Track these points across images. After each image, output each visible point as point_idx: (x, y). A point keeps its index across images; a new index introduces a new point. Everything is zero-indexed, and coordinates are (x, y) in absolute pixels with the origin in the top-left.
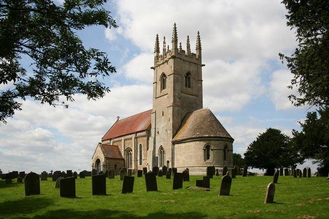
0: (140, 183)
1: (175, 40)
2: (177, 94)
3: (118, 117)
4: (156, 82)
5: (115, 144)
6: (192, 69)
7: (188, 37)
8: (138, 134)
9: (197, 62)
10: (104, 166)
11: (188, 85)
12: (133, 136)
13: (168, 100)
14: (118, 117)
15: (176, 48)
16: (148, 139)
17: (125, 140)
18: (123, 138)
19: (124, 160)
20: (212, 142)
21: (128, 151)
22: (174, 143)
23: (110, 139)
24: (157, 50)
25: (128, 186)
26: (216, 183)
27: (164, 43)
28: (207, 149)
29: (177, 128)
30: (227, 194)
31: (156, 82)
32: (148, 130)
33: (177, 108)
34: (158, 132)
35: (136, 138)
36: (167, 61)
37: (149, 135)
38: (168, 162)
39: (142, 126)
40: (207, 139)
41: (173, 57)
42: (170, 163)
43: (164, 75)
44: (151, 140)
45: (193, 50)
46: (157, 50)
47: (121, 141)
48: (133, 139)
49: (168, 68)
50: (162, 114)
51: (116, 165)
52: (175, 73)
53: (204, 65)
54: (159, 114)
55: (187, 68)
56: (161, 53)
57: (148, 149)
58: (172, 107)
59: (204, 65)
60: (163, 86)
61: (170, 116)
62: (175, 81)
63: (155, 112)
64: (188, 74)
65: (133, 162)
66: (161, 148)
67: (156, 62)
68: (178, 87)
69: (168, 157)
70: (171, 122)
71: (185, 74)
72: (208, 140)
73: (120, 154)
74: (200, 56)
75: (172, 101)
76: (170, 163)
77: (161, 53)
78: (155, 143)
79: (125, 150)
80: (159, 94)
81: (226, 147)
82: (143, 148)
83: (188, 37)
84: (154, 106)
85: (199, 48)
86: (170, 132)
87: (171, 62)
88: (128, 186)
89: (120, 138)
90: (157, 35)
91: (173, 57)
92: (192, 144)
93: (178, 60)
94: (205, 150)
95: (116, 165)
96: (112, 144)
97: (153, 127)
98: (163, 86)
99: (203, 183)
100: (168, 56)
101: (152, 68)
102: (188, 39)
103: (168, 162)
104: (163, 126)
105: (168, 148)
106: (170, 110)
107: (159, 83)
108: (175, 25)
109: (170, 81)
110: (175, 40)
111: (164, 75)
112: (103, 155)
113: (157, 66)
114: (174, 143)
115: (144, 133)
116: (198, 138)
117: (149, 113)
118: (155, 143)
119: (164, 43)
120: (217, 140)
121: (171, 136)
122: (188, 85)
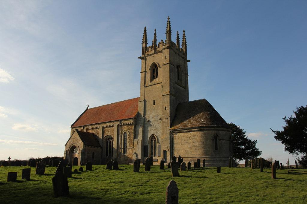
1: (169, 33)
2: (172, 83)
3: (88, 106)
4: (145, 72)
5: (90, 131)
6: (182, 63)
7: (178, 32)
11: (179, 78)
12: (116, 124)
14: (88, 106)
17: (103, 128)
18: (101, 126)
19: (101, 147)
23: (84, 127)
24: (145, 41)
28: (215, 138)
31: (145, 72)
33: (173, 97)
37: (136, 125)
38: (165, 152)
40: (216, 128)
47: (98, 128)
48: (116, 127)
49: (162, 58)
50: (153, 103)
51: (93, 153)
53: (189, 61)
54: (149, 104)
58: (169, 96)
59: (189, 61)
63: (145, 101)
66: (153, 137)
70: (168, 110)
75: (168, 89)
76: (168, 154)
82: (128, 136)
83: (178, 32)
84: (141, 95)
85: (185, 44)
86: (167, 122)
87: (166, 52)
89: (98, 126)
90: (145, 28)
91: (168, 48)
93: (173, 51)
94: (213, 140)
95: (93, 153)
96: (85, 131)
101: (140, 58)
102: (178, 34)
103: (165, 152)
106: (167, 99)
108: (169, 19)
110: (169, 33)
112: (81, 141)
114: (172, 133)
115: (131, 121)
120: (225, 131)
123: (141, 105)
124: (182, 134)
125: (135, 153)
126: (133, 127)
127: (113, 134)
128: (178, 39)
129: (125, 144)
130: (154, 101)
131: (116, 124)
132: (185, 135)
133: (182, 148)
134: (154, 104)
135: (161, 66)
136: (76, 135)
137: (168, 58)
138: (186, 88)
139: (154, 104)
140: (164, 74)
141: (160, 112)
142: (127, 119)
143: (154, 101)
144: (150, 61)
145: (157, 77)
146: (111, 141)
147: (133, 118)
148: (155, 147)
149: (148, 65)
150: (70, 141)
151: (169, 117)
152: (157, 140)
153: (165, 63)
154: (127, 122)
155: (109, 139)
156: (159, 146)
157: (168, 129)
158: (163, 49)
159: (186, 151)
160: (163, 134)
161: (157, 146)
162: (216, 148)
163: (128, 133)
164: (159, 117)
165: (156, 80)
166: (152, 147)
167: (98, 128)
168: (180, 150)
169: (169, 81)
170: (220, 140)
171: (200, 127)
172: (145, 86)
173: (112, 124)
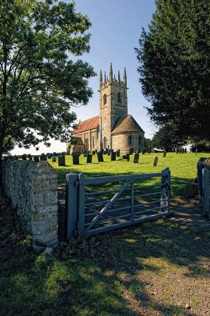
0: (95, 158)
1: (111, 73)
4: (101, 100)
5: (79, 136)
6: (122, 91)
9: (124, 86)
10: (74, 149)
11: (119, 101)
12: (89, 131)
13: (107, 110)
15: (112, 79)
16: (97, 133)
18: (83, 133)
20: (133, 134)
21: (86, 141)
22: (112, 135)
25: (89, 161)
26: (132, 157)
27: (105, 75)
29: (113, 127)
30: (137, 162)
31: (101, 100)
32: (98, 128)
33: (113, 115)
35: (91, 133)
36: (107, 87)
37: (98, 132)
39: (95, 125)
41: (110, 84)
42: (110, 147)
43: (105, 95)
44: (99, 134)
45: (122, 80)
46: (101, 80)
47: (82, 134)
49: (107, 91)
52: (111, 94)
55: (118, 90)
56: (103, 82)
60: (105, 102)
61: (109, 120)
62: (112, 99)
64: (119, 94)
65: (89, 147)
67: (100, 88)
68: (114, 103)
69: (108, 143)
71: (117, 94)
74: (126, 83)
75: (110, 111)
76: (110, 147)
77: (103, 82)
78: (101, 135)
79: (85, 140)
80: (103, 107)
81: (140, 137)
85: (125, 78)
86: (110, 129)
87: (109, 87)
88: (89, 161)
91: (110, 84)
92: (122, 136)
97: (100, 126)
98: (105, 102)
99: (127, 157)
100: (108, 84)
104: (106, 125)
105: (108, 138)
106: (110, 116)
107: (103, 99)
109: (109, 99)
110: (111, 73)
111: (105, 95)
114: (112, 135)
117: (97, 118)
118: (101, 135)
119: (105, 75)
122: (119, 101)
123: (100, 120)
124: (115, 136)
128: (119, 76)
129: (93, 143)
138: (125, 107)
154: (94, 130)
167: (82, 134)
171: (122, 132)
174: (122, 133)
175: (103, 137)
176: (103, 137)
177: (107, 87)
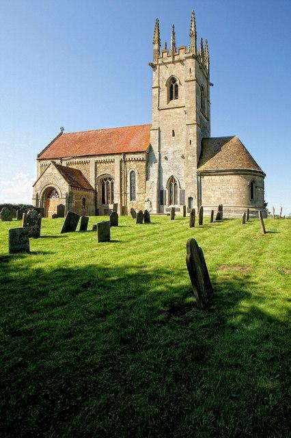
3: (62, 129)
5: (74, 167)
8: (128, 157)
12: (118, 159)
14: (62, 129)
18: (93, 160)
19: (95, 191)
21: (105, 181)
22: (201, 175)
34: (166, 158)
35: (124, 161)
36: (181, 61)
38: (190, 199)
42: (195, 202)
44: (154, 168)
47: (88, 163)
50: (171, 134)
57: (147, 179)
63: (159, 129)
66: (172, 179)
70: (194, 145)
72: (254, 175)
73: (88, 183)
76: (195, 202)
79: (96, 178)
86: (193, 159)
87: (191, 63)
97: (156, 150)
103: (190, 199)
113: (160, 65)
114: (201, 175)
115: (142, 156)
116: (246, 170)
121: (196, 165)
123: (154, 134)
124: (213, 177)
125: (148, 200)
126: (145, 164)
127: (114, 173)
129: (132, 187)
130: (173, 131)
131: (118, 159)
132: (217, 178)
133: (213, 195)
134: (174, 135)
135: (183, 83)
136: (53, 171)
137: (193, 73)
139: (174, 135)
140: (187, 94)
141: (182, 146)
142: (134, 153)
143: (173, 131)
144: (166, 73)
145: (176, 98)
146: (110, 182)
147: (143, 152)
148: (176, 192)
149: (163, 78)
150: (42, 179)
151: (195, 155)
152: (177, 183)
153: (188, 78)
154: (136, 156)
155: (106, 179)
156: (183, 192)
157: (195, 170)
158: (187, 58)
159: (219, 199)
160: (187, 175)
161: (179, 192)
162: (252, 197)
163: (136, 172)
164: (181, 154)
165: (174, 102)
166: (171, 192)
167: (88, 163)
168: (210, 197)
169: (195, 105)
170: (256, 187)
171: (237, 170)
172: (159, 110)
173: (111, 158)
174: (236, 172)
175: (166, 177)
176: (166, 177)
177: (181, 61)
